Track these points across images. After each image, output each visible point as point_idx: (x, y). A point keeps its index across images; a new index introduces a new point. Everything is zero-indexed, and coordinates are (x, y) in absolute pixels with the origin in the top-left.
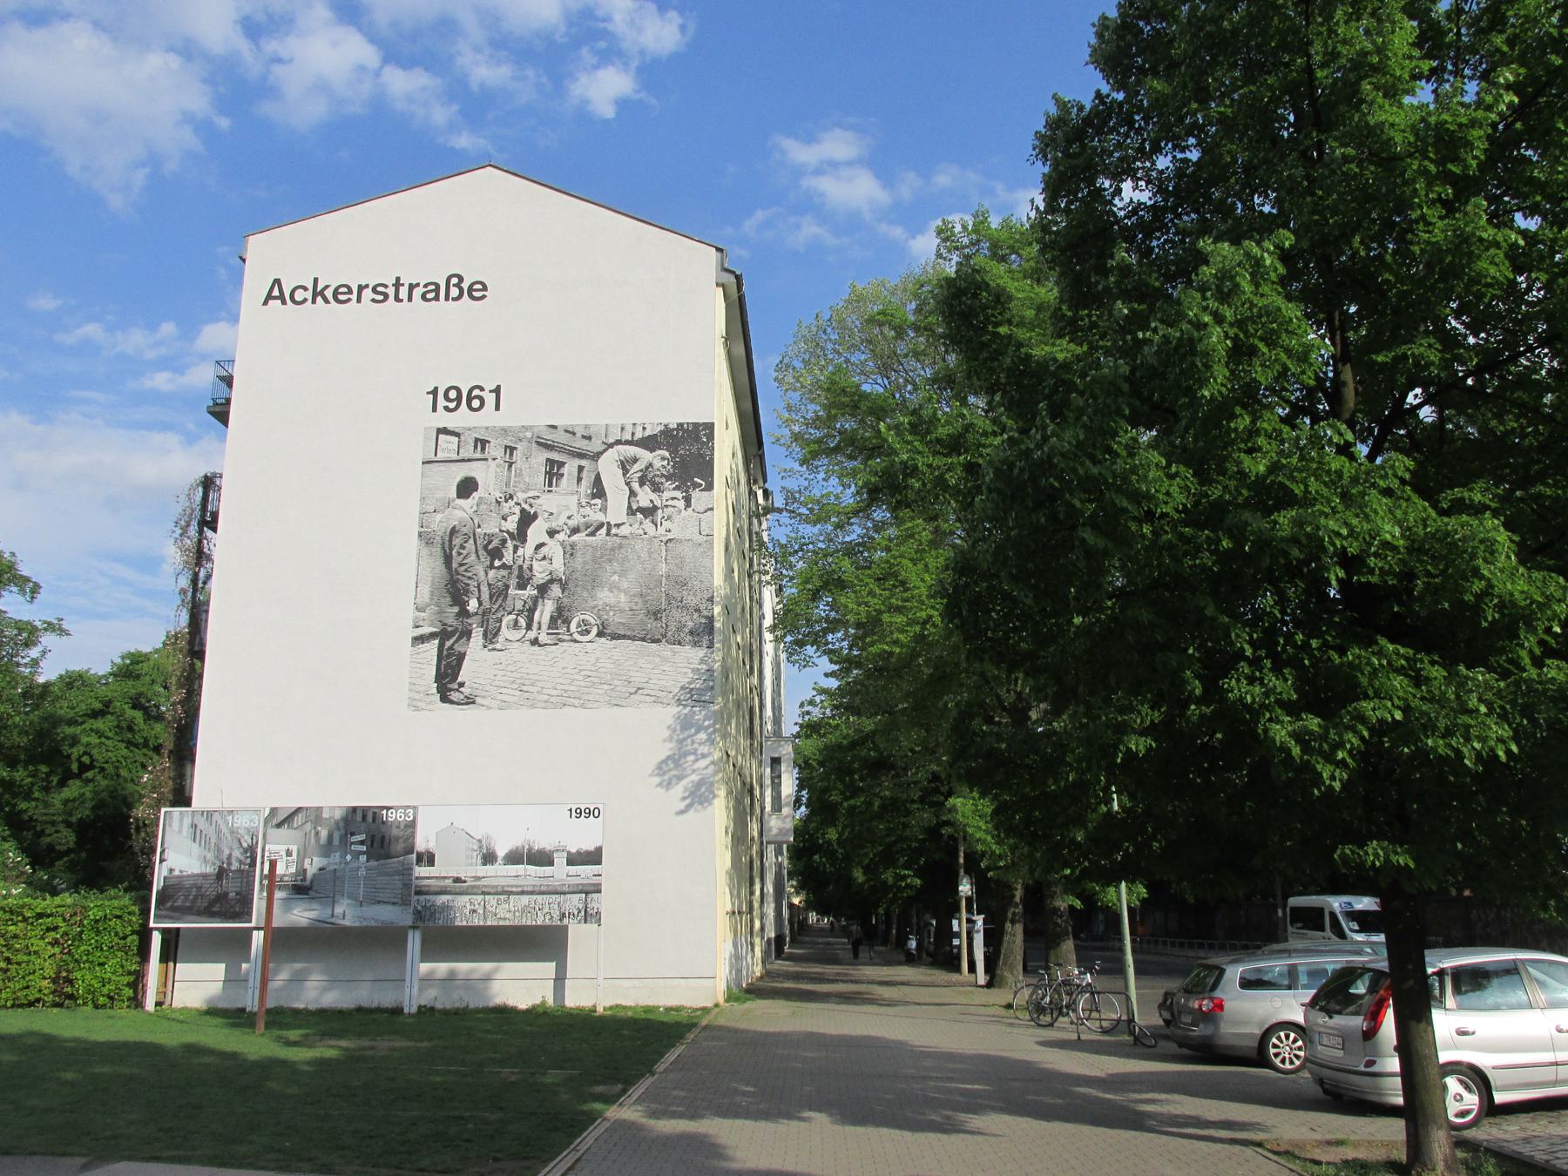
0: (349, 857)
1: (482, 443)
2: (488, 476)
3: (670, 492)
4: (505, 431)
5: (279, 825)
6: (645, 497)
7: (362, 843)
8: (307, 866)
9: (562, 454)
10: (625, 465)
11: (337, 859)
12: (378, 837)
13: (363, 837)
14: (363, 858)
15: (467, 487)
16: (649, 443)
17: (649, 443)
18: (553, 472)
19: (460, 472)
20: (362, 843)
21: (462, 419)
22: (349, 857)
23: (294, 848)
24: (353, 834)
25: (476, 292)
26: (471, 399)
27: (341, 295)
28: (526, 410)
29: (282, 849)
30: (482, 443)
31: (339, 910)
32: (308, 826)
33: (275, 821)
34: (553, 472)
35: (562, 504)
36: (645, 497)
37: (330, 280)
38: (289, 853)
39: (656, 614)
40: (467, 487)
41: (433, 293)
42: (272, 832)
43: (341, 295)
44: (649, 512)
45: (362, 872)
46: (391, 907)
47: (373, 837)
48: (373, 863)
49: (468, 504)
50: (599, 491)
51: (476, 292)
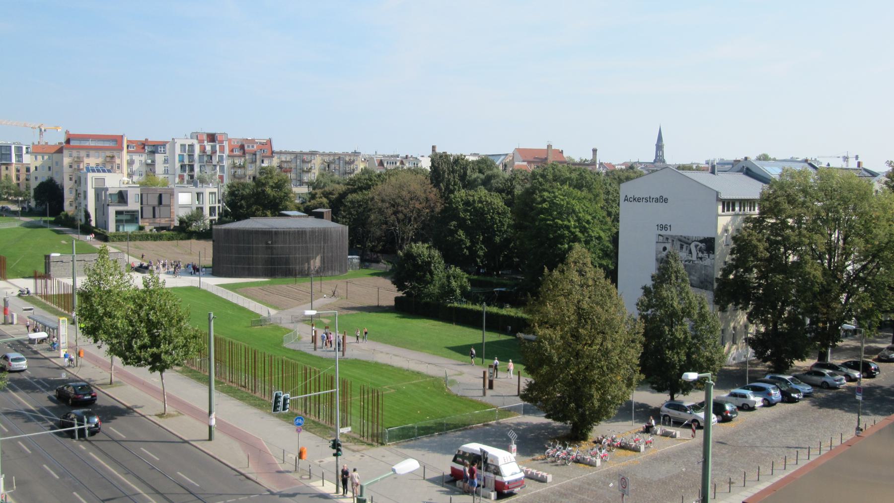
1: (667, 239)
2: (668, 246)
3: (706, 255)
4: (672, 236)
6: (700, 255)
9: (684, 242)
10: (696, 246)
15: (665, 249)
16: (701, 241)
17: (701, 241)
18: (682, 247)
19: (663, 245)
21: (663, 232)
25: (666, 200)
26: (663, 227)
27: (639, 200)
28: (675, 232)
30: (667, 239)
34: (682, 247)
35: (683, 255)
36: (700, 255)
37: (637, 196)
39: (702, 282)
40: (665, 249)
41: (657, 200)
43: (639, 200)
44: (701, 258)
49: (665, 253)
50: (690, 252)
51: (666, 200)
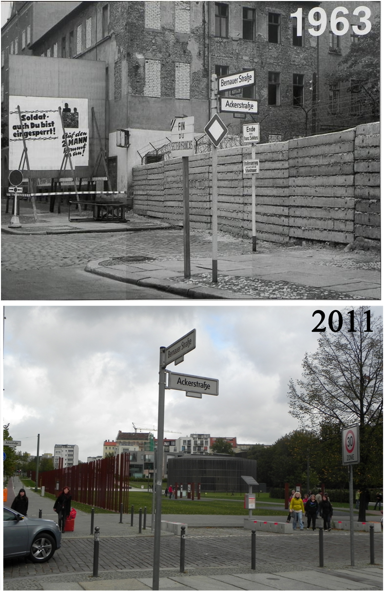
0: (216, 130)
5: (38, 48)
7: (247, 92)
8: (114, 150)
11: (190, 135)
12: (286, 80)
13: (247, 79)
14: (252, 131)
20: (247, 92)
22: (216, 130)
23: (81, 106)
24: (222, 71)
29: (50, 106)
31: (201, 262)
32: (112, 52)
33: (30, 36)
38: (69, 118)
42: (25, 67)
45: (252, 166)
46: (326, 255)
47: (273, 77)
48: (276, 144)
